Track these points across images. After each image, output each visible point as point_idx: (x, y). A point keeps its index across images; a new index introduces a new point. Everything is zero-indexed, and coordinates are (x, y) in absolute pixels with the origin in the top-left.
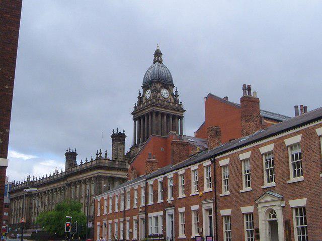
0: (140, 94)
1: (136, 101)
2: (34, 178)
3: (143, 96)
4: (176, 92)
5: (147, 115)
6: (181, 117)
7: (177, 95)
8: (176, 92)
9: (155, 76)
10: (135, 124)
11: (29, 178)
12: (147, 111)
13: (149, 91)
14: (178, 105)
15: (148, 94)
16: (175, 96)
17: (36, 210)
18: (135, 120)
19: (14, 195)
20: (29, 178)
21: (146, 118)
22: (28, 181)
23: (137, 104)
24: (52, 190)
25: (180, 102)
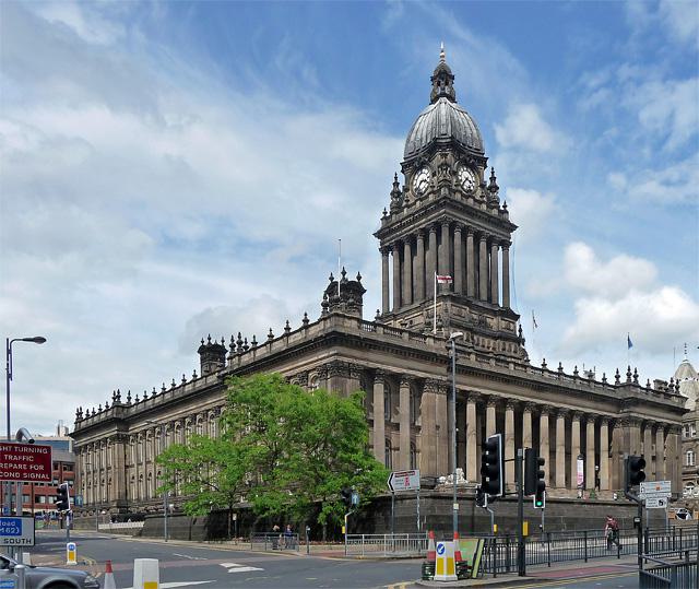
0: (396, 184)
1: (387, 202)
2: (129, 398)
3: (406, 190)
4: (493, 179)
5: (425, 233)
6: (506, 244)
7: (494, 188)
8: (493, 179)
9: (443, 131)
10: (386, 262)
11: (117, 397)
12: (423, 223)
13: (425, 174)
14: (500, 211)
15: (423, 179)
16: (490, 188)
17: (142, 471)
18: (385, 251)
19: (84, 441)
20: (117, 397)
21: (420, 242)
22: (117, 405)
23: (388, 210)
24: (183, 420)
25: (501, 204)
